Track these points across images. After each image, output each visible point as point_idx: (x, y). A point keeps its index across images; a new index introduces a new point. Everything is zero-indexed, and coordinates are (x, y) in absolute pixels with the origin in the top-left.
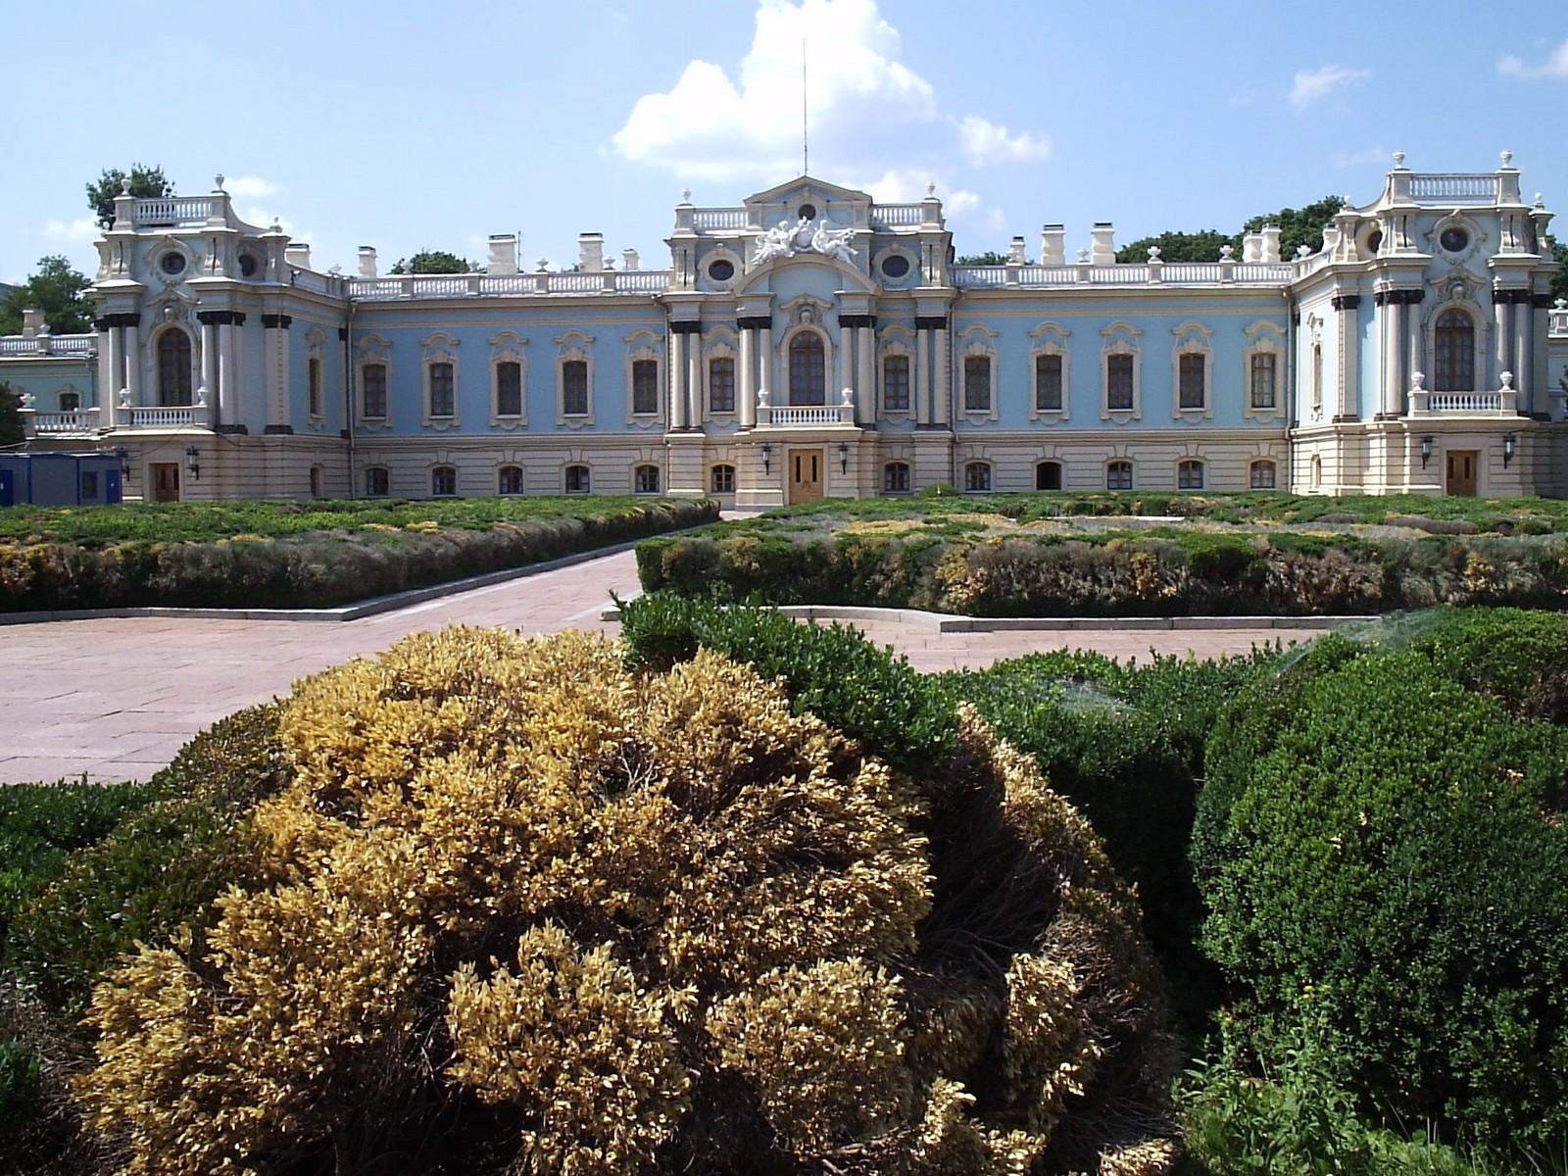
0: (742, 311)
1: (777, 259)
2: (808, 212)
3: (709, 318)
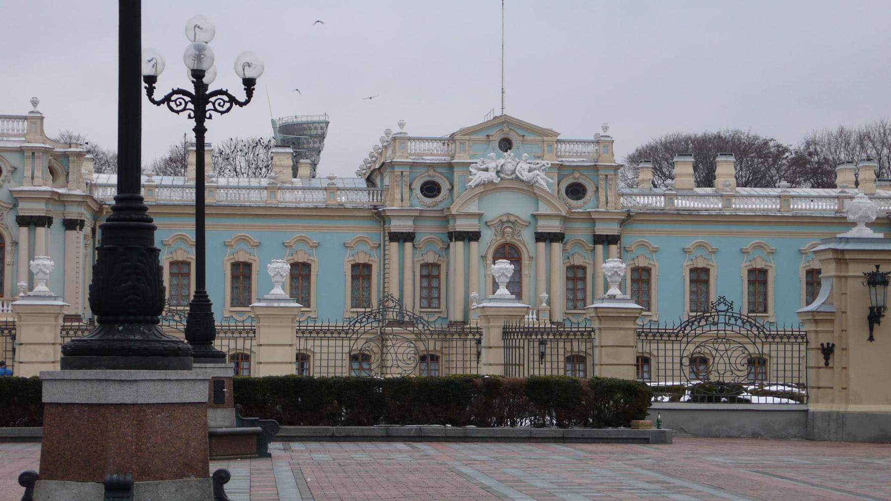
1: (483, 184)
2: (506, 145)
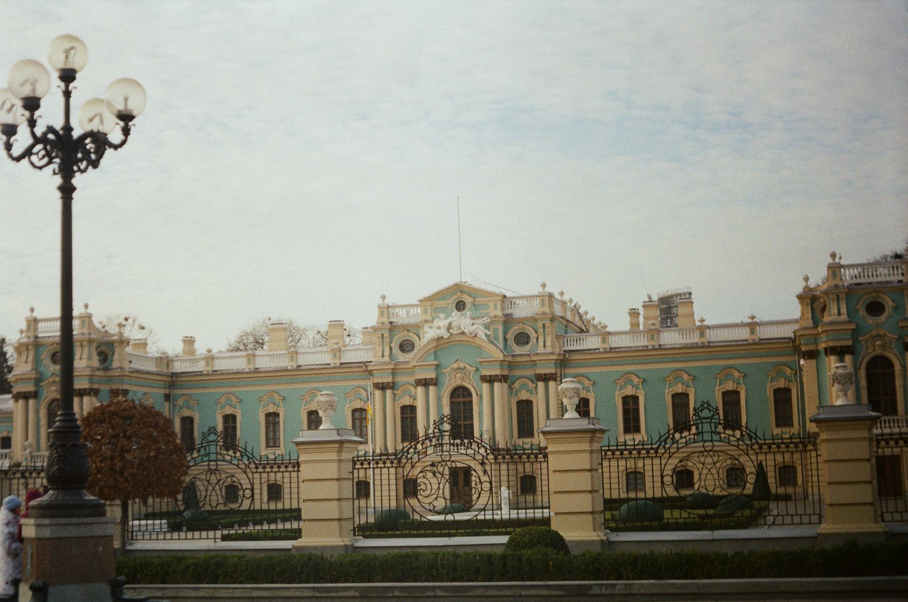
2: (460, 306)
3: (399, 379)
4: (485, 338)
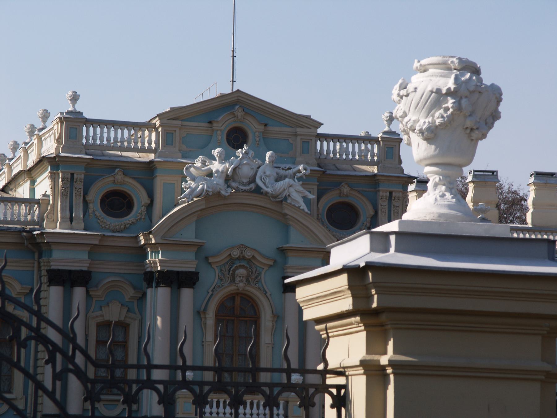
0: (156, 260)
4: (303, 206)
